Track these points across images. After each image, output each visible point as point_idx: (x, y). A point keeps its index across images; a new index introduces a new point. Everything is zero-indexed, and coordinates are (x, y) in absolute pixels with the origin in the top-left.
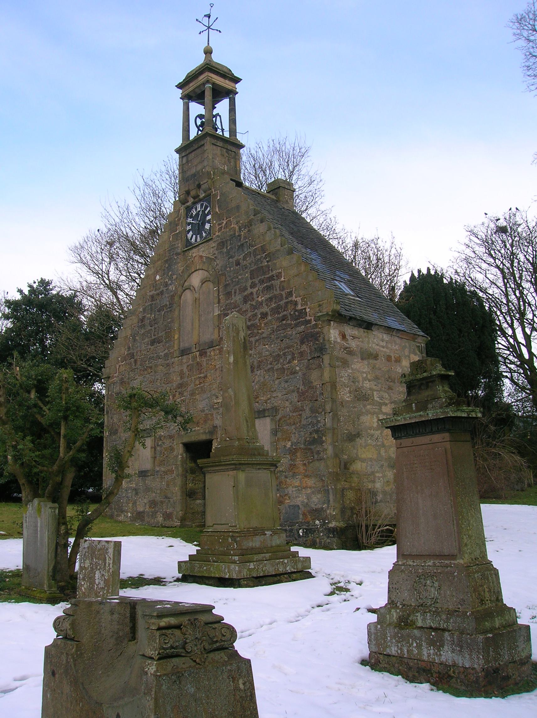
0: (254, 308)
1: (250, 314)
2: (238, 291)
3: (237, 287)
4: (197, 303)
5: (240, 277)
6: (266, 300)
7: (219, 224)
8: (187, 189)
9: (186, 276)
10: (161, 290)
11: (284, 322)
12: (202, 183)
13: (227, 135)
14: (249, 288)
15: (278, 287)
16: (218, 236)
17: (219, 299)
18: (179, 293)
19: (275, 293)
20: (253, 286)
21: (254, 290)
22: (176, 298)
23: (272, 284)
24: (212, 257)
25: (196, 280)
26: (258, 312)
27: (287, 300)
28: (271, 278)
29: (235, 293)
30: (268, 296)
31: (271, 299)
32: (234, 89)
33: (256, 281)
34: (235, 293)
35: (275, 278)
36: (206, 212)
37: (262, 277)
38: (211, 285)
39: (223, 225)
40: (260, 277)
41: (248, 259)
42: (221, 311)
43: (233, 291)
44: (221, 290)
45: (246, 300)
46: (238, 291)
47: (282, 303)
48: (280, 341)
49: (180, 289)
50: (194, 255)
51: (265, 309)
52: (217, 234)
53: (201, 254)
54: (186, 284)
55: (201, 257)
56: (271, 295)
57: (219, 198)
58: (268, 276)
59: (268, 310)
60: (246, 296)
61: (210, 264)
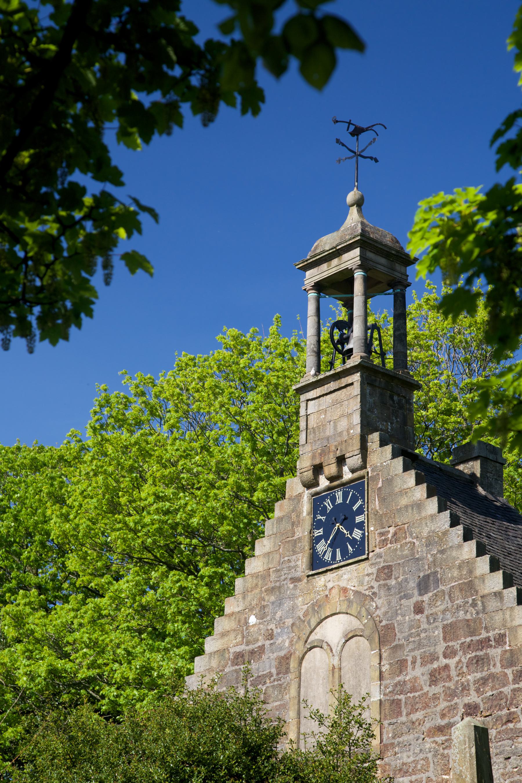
0: (451, 694)
1: (443, 705)
2: (419, 661)
3: (417, 653)
4: (337, 675)
5: (423, 635)
6: (475, 682)
7: (382, 534)
8: (317, 462)
9: (313, 623)
10: (260, 644)
11: (511, 725)
12: (347, 455)
13: (390, 364)
14: (441, 656)
15: (498, 660)
16: (379, 556)
17: (381, 672)
18: (299, 654)
19: (493, 670)
20: (449, 653)
21: (452, 662)
22: (293, 664)
23: (487, 654)
24: (367, 593)
25: (333, 630)
26: (461, 702)
27: (517, 686)
28: (485, 643)
29: (414, 662)
30: (479, 675)
31: (484, 681)
32: (405, 277)
33: (456, 645)
34: (414, 662)
35: (493, 643)
36: (355, 508)
37: (468, 639)
38: (363, 642)
39: (390, 536)
40: (463, 640)
41: (439, 603)
42: (384, 695)
43: (410, 659)
44: (384, 655)
45: (434, 678)
46: (419, 661)
47: (507, 690)
48: (502, 760)
49: (300, 648)
50: (330, 585)
51: (473, 698)
52: (377, 550)
53: (343, 584)
54: (312, 638)
55: (345, 590)
56: (484, 674)
57: (380, 485)
58: (478, 638)
59: (478, 700)
60: (435, 670)
61: (363, 605)
